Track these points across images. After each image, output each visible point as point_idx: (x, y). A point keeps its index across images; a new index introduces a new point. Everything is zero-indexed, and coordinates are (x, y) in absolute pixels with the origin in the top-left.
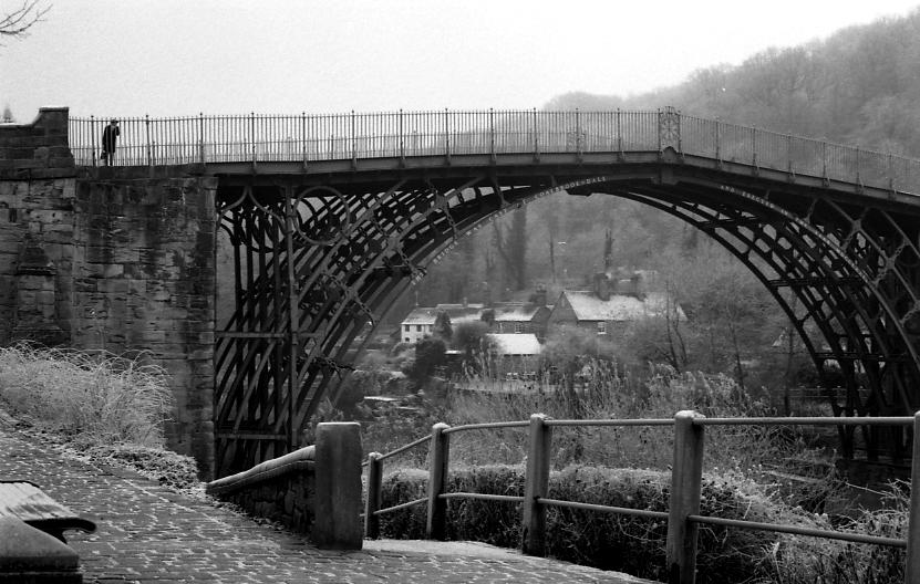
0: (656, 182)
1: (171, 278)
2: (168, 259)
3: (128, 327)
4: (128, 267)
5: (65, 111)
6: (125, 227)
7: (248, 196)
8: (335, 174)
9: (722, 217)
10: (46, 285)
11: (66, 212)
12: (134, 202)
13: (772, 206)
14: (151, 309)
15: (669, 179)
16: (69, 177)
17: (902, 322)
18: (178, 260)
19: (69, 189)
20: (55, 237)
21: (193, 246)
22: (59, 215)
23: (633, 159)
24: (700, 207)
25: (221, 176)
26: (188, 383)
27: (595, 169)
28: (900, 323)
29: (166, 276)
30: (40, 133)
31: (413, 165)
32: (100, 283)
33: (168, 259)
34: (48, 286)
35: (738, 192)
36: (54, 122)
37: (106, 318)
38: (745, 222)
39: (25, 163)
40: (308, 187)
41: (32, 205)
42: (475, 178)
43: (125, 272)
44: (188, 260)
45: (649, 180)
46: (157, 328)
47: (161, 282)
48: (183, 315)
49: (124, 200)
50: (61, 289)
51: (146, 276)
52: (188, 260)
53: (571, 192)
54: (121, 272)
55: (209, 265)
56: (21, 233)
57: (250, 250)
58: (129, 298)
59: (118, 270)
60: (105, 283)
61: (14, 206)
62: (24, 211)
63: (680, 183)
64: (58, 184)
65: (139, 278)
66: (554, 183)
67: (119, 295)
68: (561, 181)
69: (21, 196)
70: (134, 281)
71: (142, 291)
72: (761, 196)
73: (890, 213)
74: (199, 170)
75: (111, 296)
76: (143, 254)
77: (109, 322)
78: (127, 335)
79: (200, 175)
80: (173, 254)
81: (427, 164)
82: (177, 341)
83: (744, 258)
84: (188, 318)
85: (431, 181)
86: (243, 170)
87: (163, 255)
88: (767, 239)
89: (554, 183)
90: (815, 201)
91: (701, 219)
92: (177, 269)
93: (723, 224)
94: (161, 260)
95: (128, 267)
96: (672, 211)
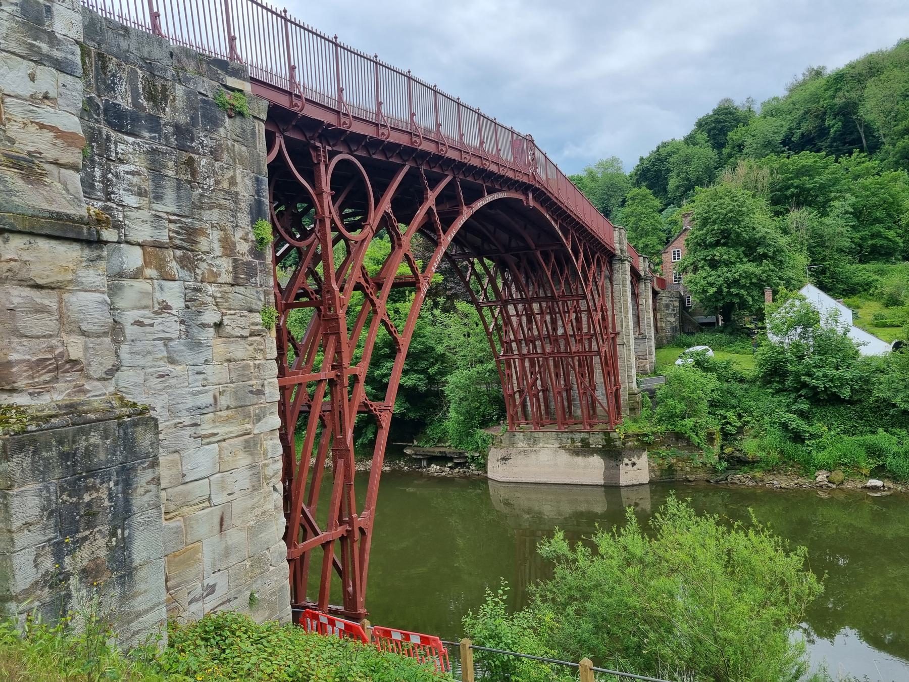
1: (220, 280)
6: (139, 163)
18: (228, 248)
22: (48, 79)
29: (213, 277)
33: (216, 235)
42: (447, 175)
43: (146, 264)
49: (135, 104)
51: (184, 274)
54: (140, 262)
59: (133, 258)
71: (177, 303)
72: (557, 224)
76: (172, 226)
87: (202, 232)
94: (203, 244)
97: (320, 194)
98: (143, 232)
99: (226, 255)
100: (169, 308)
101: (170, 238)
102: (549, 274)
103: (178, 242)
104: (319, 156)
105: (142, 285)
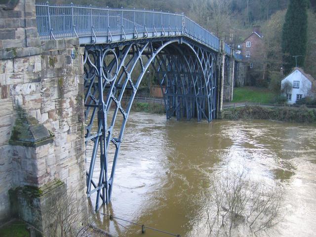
11: (37, 84)
12: (51, 67)
15: (182, 42)
22: (33, 86)
26: (79, 178)
41: (17, 81)
47: (65, 119)
49: (47, 68)
52: (75, 102)
54: (47, 118)
62: (11, 87)
64: (31, 59)
65: (56, 120)
68: (164, 42)
70: (54, 122)
71: (57, 128)
72: (192, 46)
76: (57, 103)
80: (69, 100)
82: (73, 153)
87: (65, 102)
97: (99, 67)
99: (70, 107)
100: (55, 129)
101: (56, 107)
102: (188, 64)
103: (58, 108)
104: (99, 54)
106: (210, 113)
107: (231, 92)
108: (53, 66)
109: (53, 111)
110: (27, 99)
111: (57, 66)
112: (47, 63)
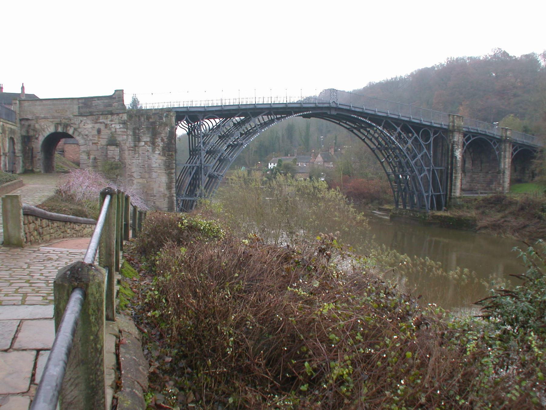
0: (329, 113)
2: (159, 140)
3: (146, 162)
4: (146, 143)
5: (123, 90)
7: (187, 118)
8: (216, 111)
9: (356, 126)
10: (116, 149)
13: (369, 122)
14: (154, 156)
15: (334, 113)
16: (124, 113)
17: (414, 162)
18: (162, 140)
19: (125, 117)
20: (120, 133)
21: (168, 135)
22: (121, 126)
23: (321, 105)
24: (347, 123)
25: (177, 112)
27: (307, 109)
28: (413, 163)
29: (159, 145)
30: (115, 98)
31: (244, 107)
32: (136, 148)
34: (118, 150)
35: (358, 117)
36: (119, 95)
37: (139, 160)
38: (362, 128)
39: (110, 109)
40: (207, 115)
42: (264, 112)
44: (166, 140)
45: (326, 113)
46: (156, 163)
48: (164, 158)
50: (122, 151)
52: (166, 140)
53: (304, 116)
55: (173, 142)
56: (109, 132)
57: (192, 136)
58: (146, 153)
59: (143, 144)
60: (138, 148)
61: (106, 123)
63: (337, 114)
64: (121, 115)
65: (149, 146)
66: (293, 113)
67: (143, 152)
68: (295, 113)
69: (109, 120)
71: (150, 150)
72: (366, 118)
73: (410, 125)
74: (169, 110)
75: (140, 152)
77: (140, 161)
78: (146, 166)
79: (170, 111)
81: (248, 107)
82: (163, 167)
83: (363, 140)
84: (166, 159)
85: (250, 113)
86: (185, 110)
87: (157, 139)
88: (371, 134)
89: (293, 113)
90: (384, 121)
91: (348, 127)
92: (162, 143)
93: (355, 128)
94: (157, 140)
95: (146, 143)
96: (339, 124)
98: (145, 140)
105: (144, 147)
106: (425, 195)
107: (504, 182)
108: (149, 120)
109: (148, 141)
110: (117, 130)
111: (151, 120)
112: (144, 119)
